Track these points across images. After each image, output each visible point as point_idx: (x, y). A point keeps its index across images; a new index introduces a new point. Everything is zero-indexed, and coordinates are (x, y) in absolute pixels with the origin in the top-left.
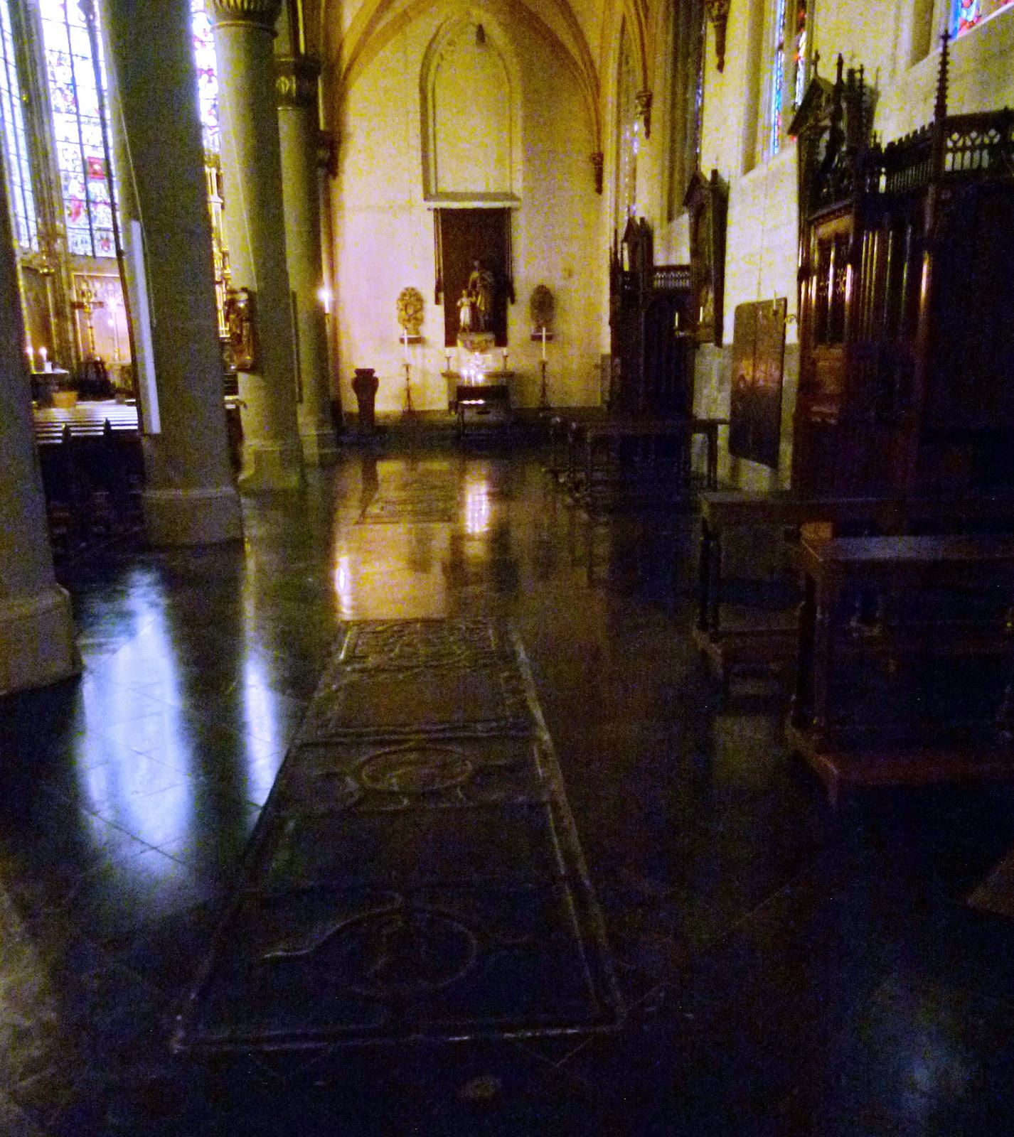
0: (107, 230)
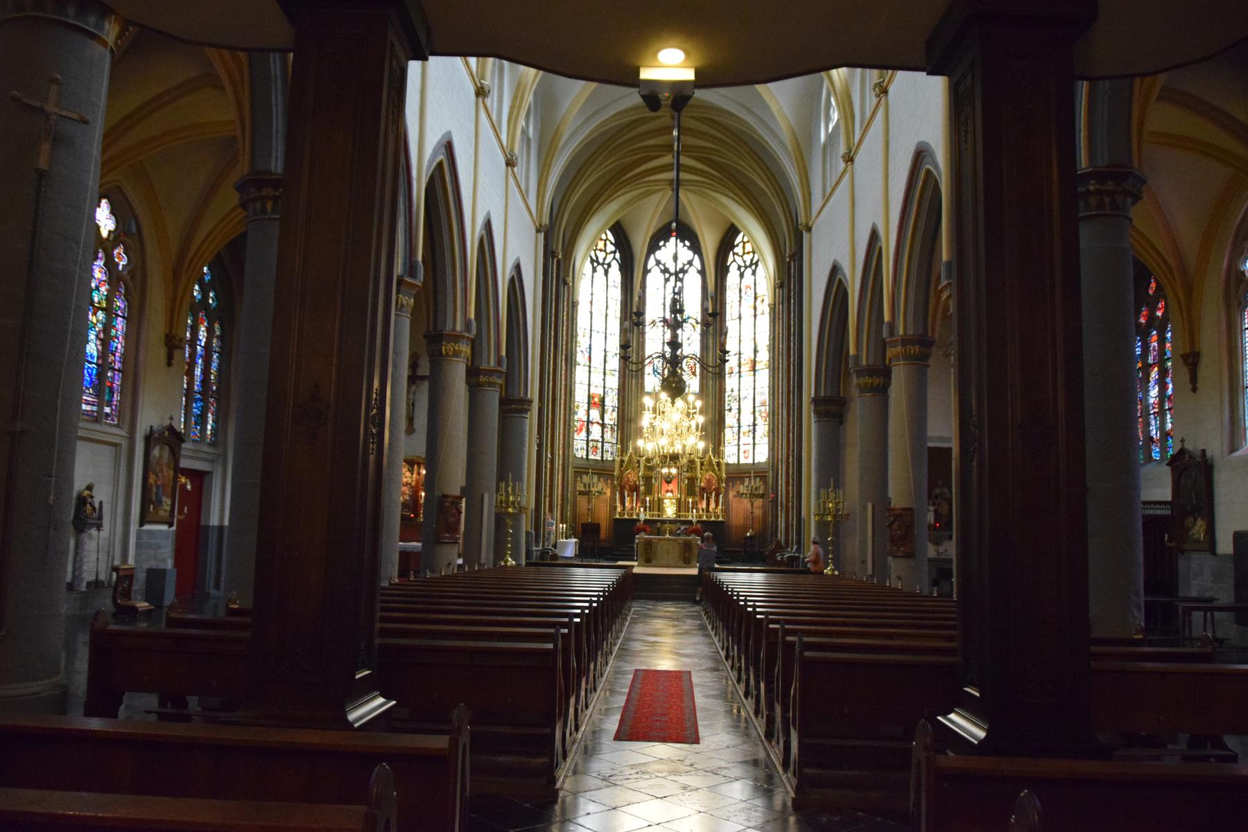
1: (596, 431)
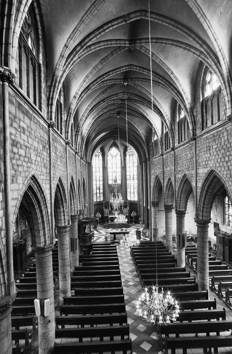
1: (98, 195)
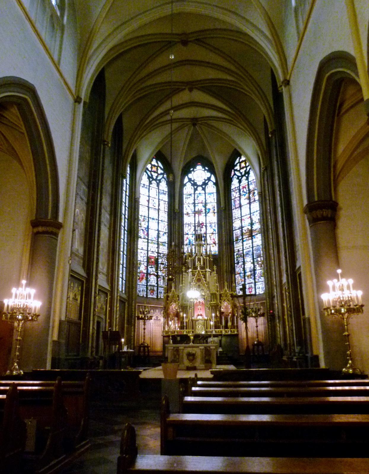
0: (154, 286)
1: (153, 280)
